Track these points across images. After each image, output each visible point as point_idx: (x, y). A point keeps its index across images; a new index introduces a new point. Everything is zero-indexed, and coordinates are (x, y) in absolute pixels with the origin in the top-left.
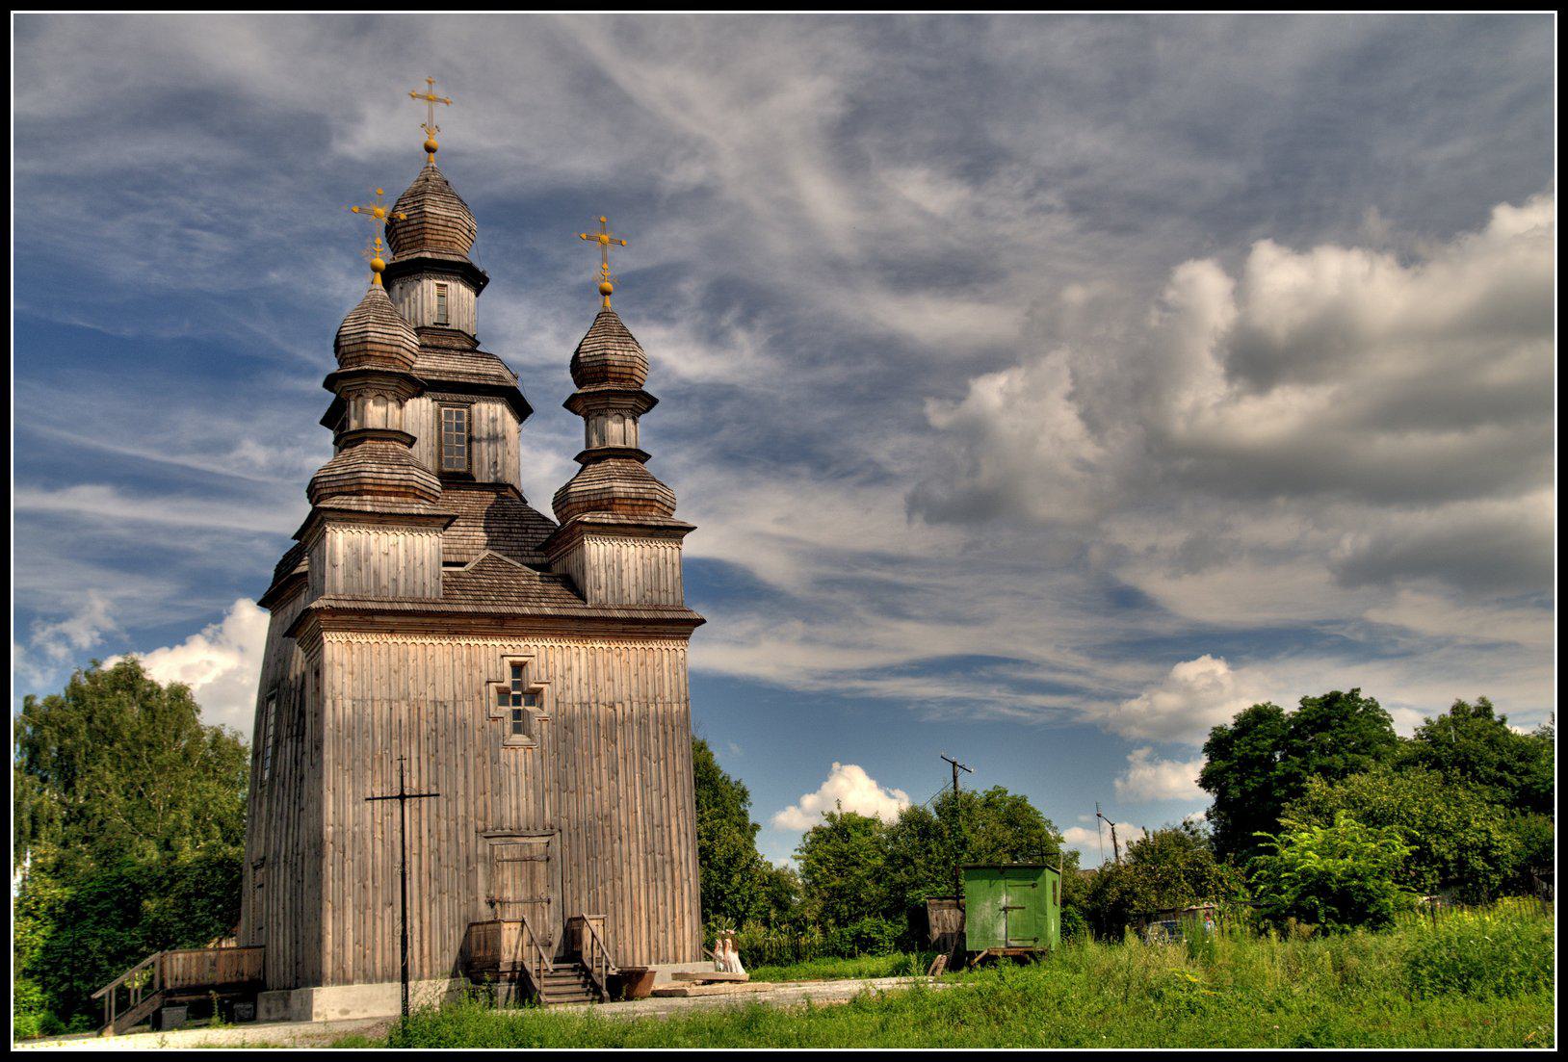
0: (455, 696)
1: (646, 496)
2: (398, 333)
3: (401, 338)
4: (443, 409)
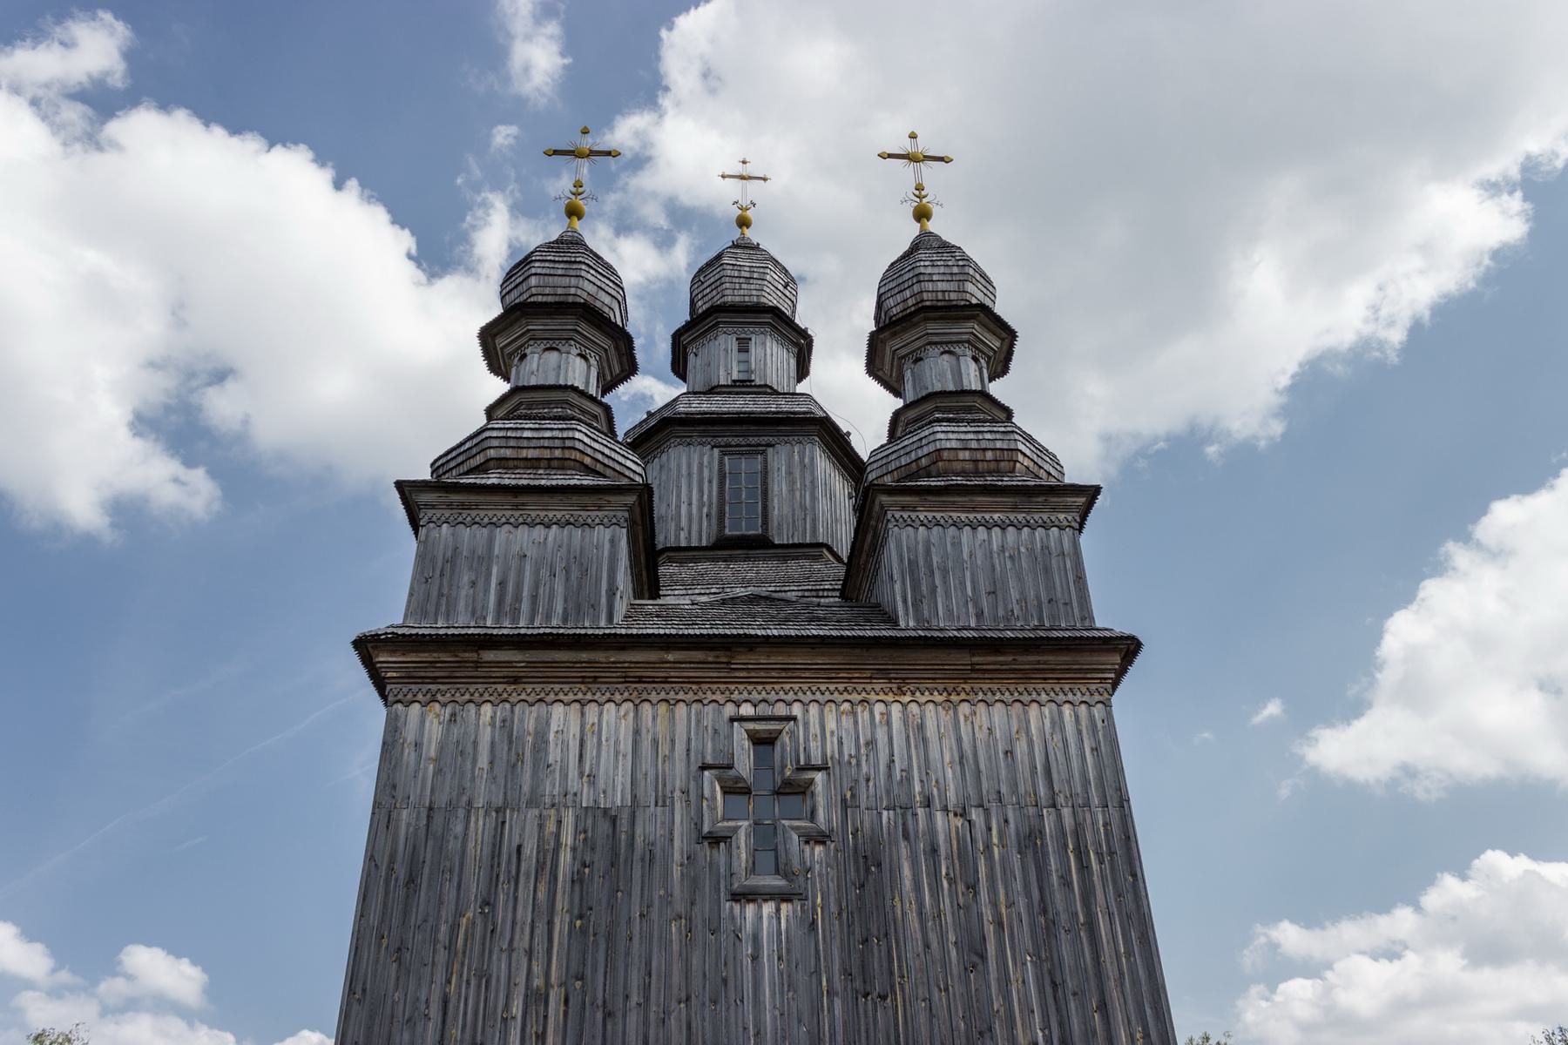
0: (634, 797)
1: (999, 445)
2: (578, 259)
3: (584, 267)
4: (726, 458)
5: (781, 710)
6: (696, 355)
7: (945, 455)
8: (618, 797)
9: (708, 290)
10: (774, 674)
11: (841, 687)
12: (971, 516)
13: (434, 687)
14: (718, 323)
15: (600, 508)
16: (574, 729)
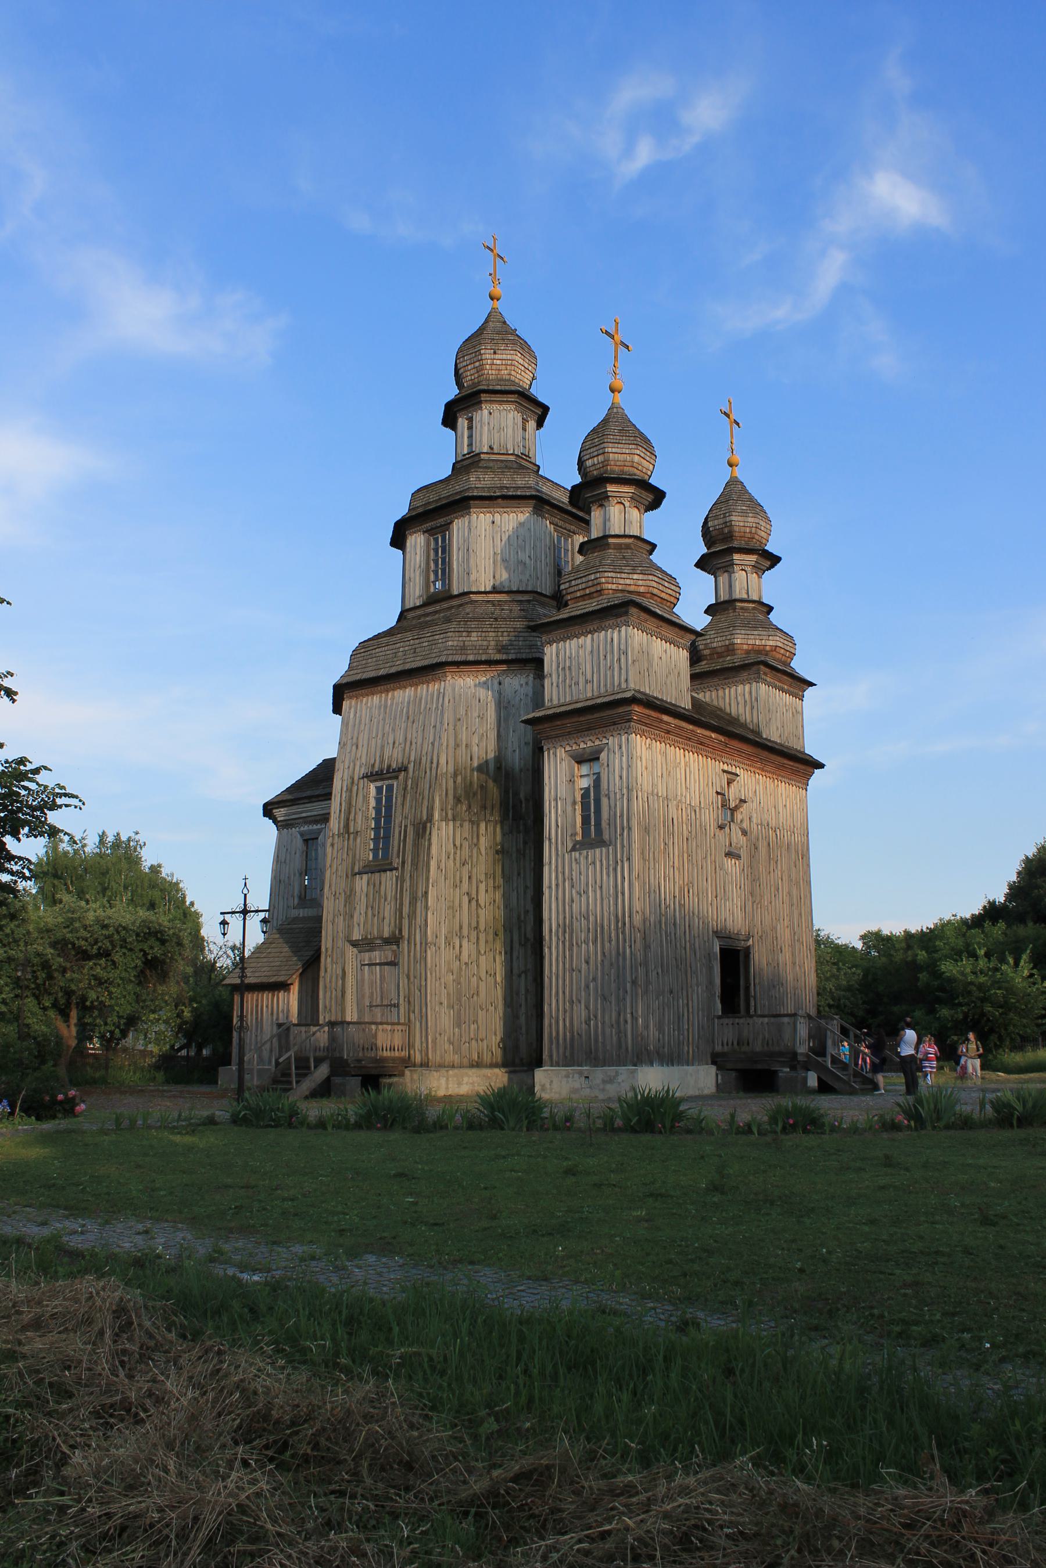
13: (645, 728)
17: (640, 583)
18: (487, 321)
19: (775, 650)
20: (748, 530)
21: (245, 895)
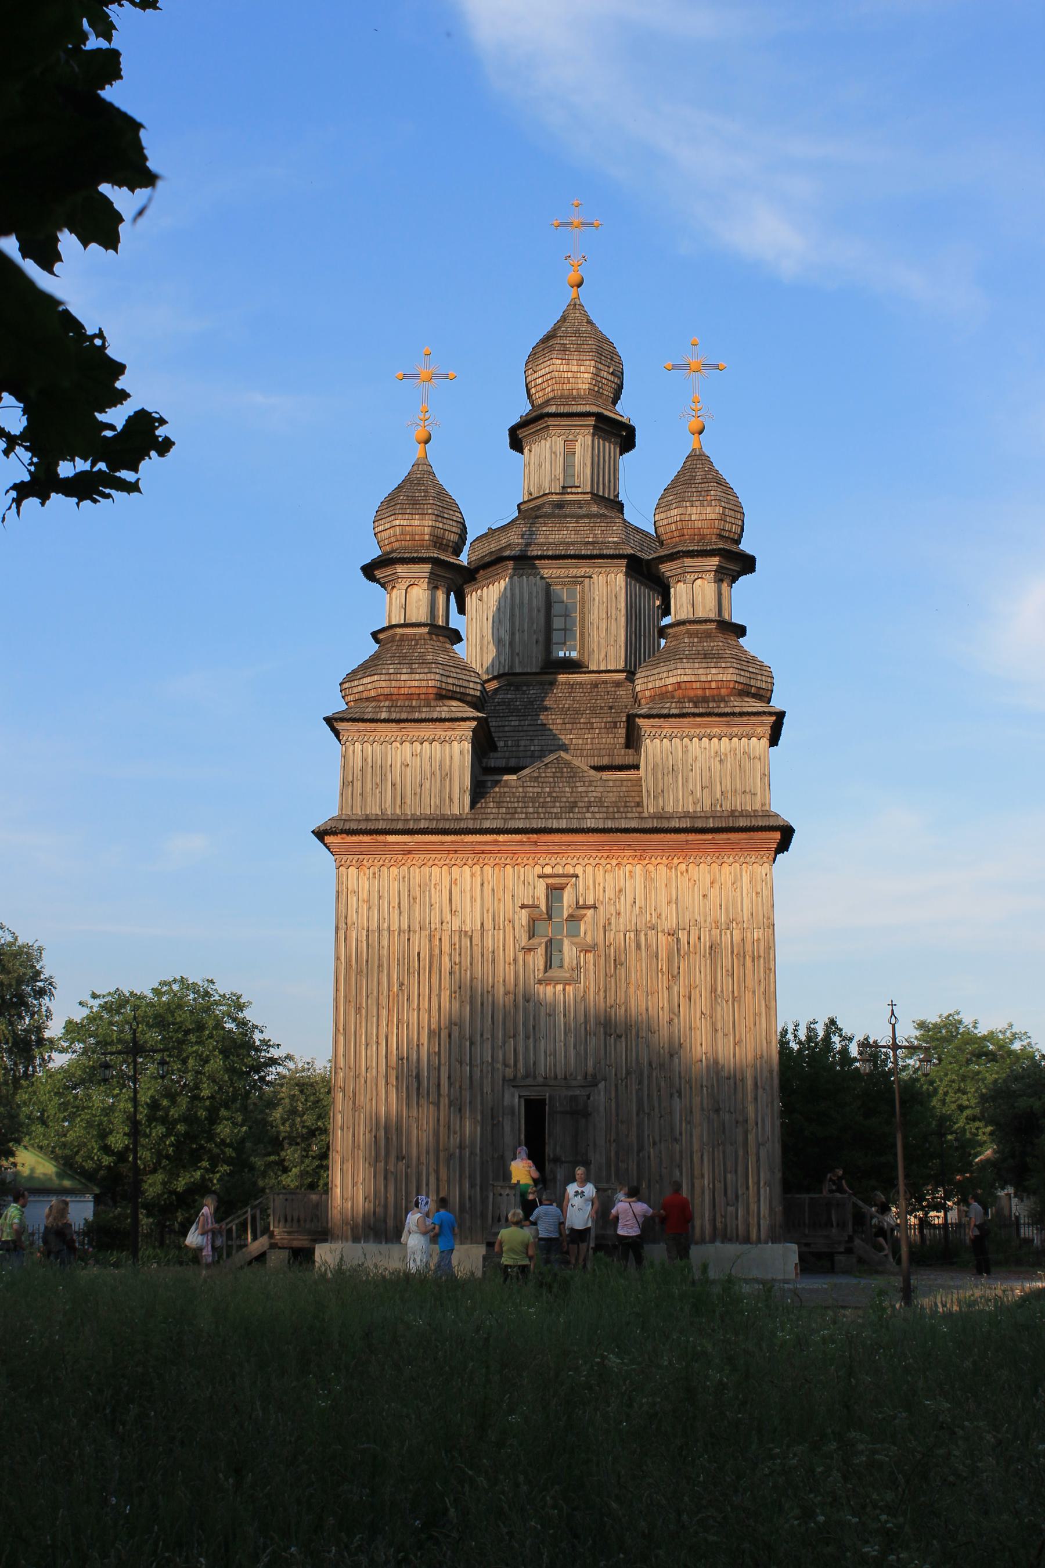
5: (570, 870)
6: (530, 451)
7: (683, 686)
8: (472, 924)
9: (540, 381)
10: (564, 848)
11: (605, 855)
12: (698, 731)
14: (548, 426)
15: (453, 729)
16: (446, 882)
17: (369, 686)
18: (564, 319)
19: (680, 688)
20: (673, 527)
21: (894, 1026)
